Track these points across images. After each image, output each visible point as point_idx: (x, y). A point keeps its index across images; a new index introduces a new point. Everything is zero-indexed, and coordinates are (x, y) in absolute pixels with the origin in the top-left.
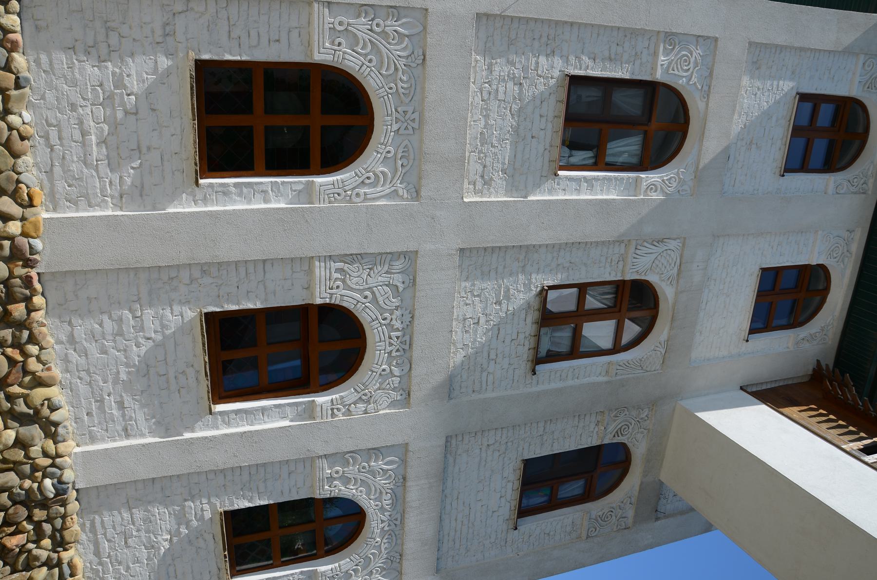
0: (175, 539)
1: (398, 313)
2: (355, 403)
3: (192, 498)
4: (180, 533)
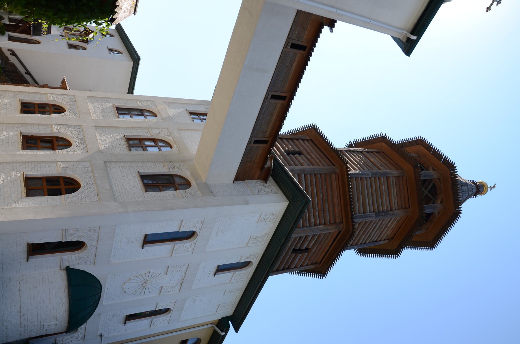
0: (5, 181)
1: (78, 136)
2: (69, 151)
3: (13, 170)
4: (7, 179)
